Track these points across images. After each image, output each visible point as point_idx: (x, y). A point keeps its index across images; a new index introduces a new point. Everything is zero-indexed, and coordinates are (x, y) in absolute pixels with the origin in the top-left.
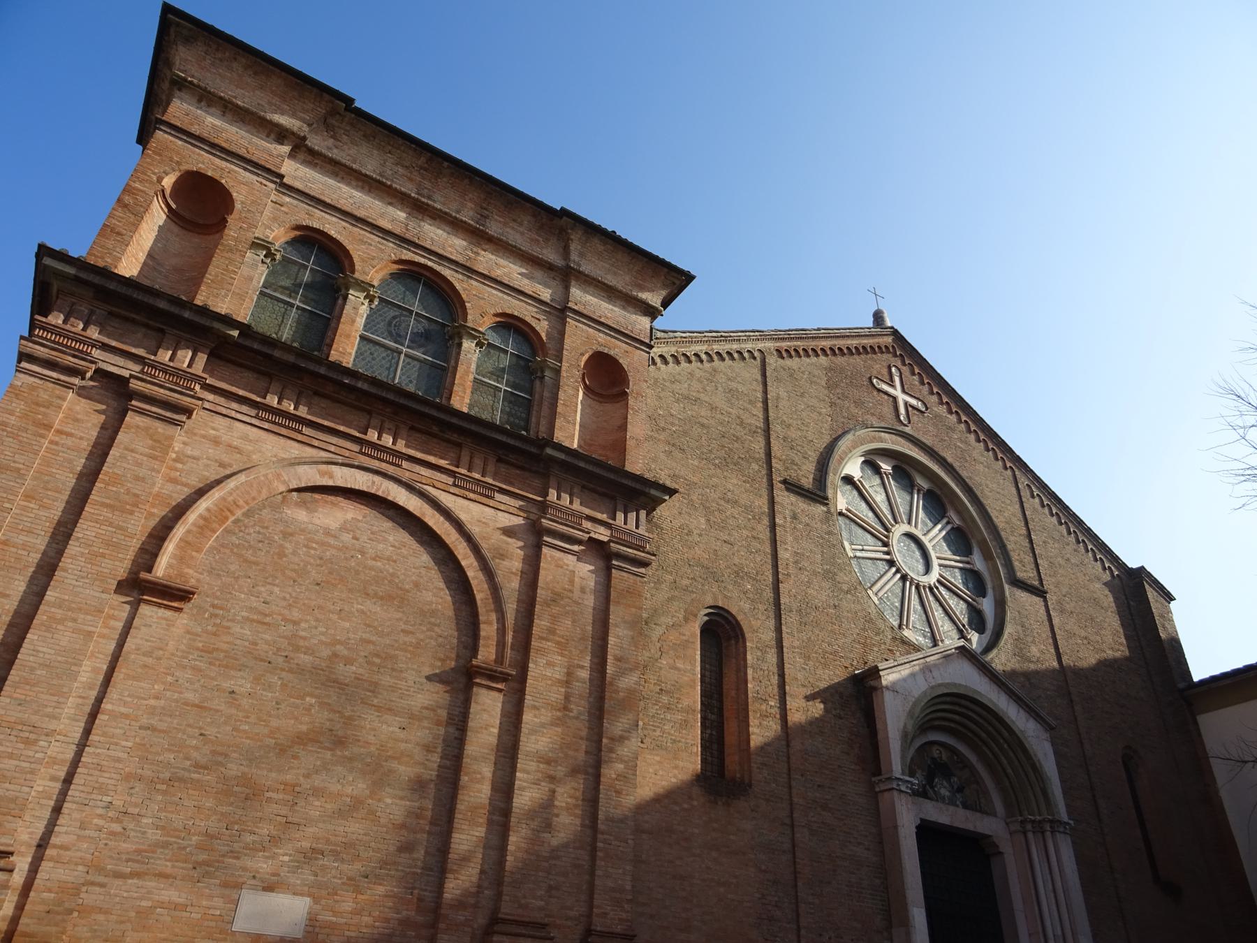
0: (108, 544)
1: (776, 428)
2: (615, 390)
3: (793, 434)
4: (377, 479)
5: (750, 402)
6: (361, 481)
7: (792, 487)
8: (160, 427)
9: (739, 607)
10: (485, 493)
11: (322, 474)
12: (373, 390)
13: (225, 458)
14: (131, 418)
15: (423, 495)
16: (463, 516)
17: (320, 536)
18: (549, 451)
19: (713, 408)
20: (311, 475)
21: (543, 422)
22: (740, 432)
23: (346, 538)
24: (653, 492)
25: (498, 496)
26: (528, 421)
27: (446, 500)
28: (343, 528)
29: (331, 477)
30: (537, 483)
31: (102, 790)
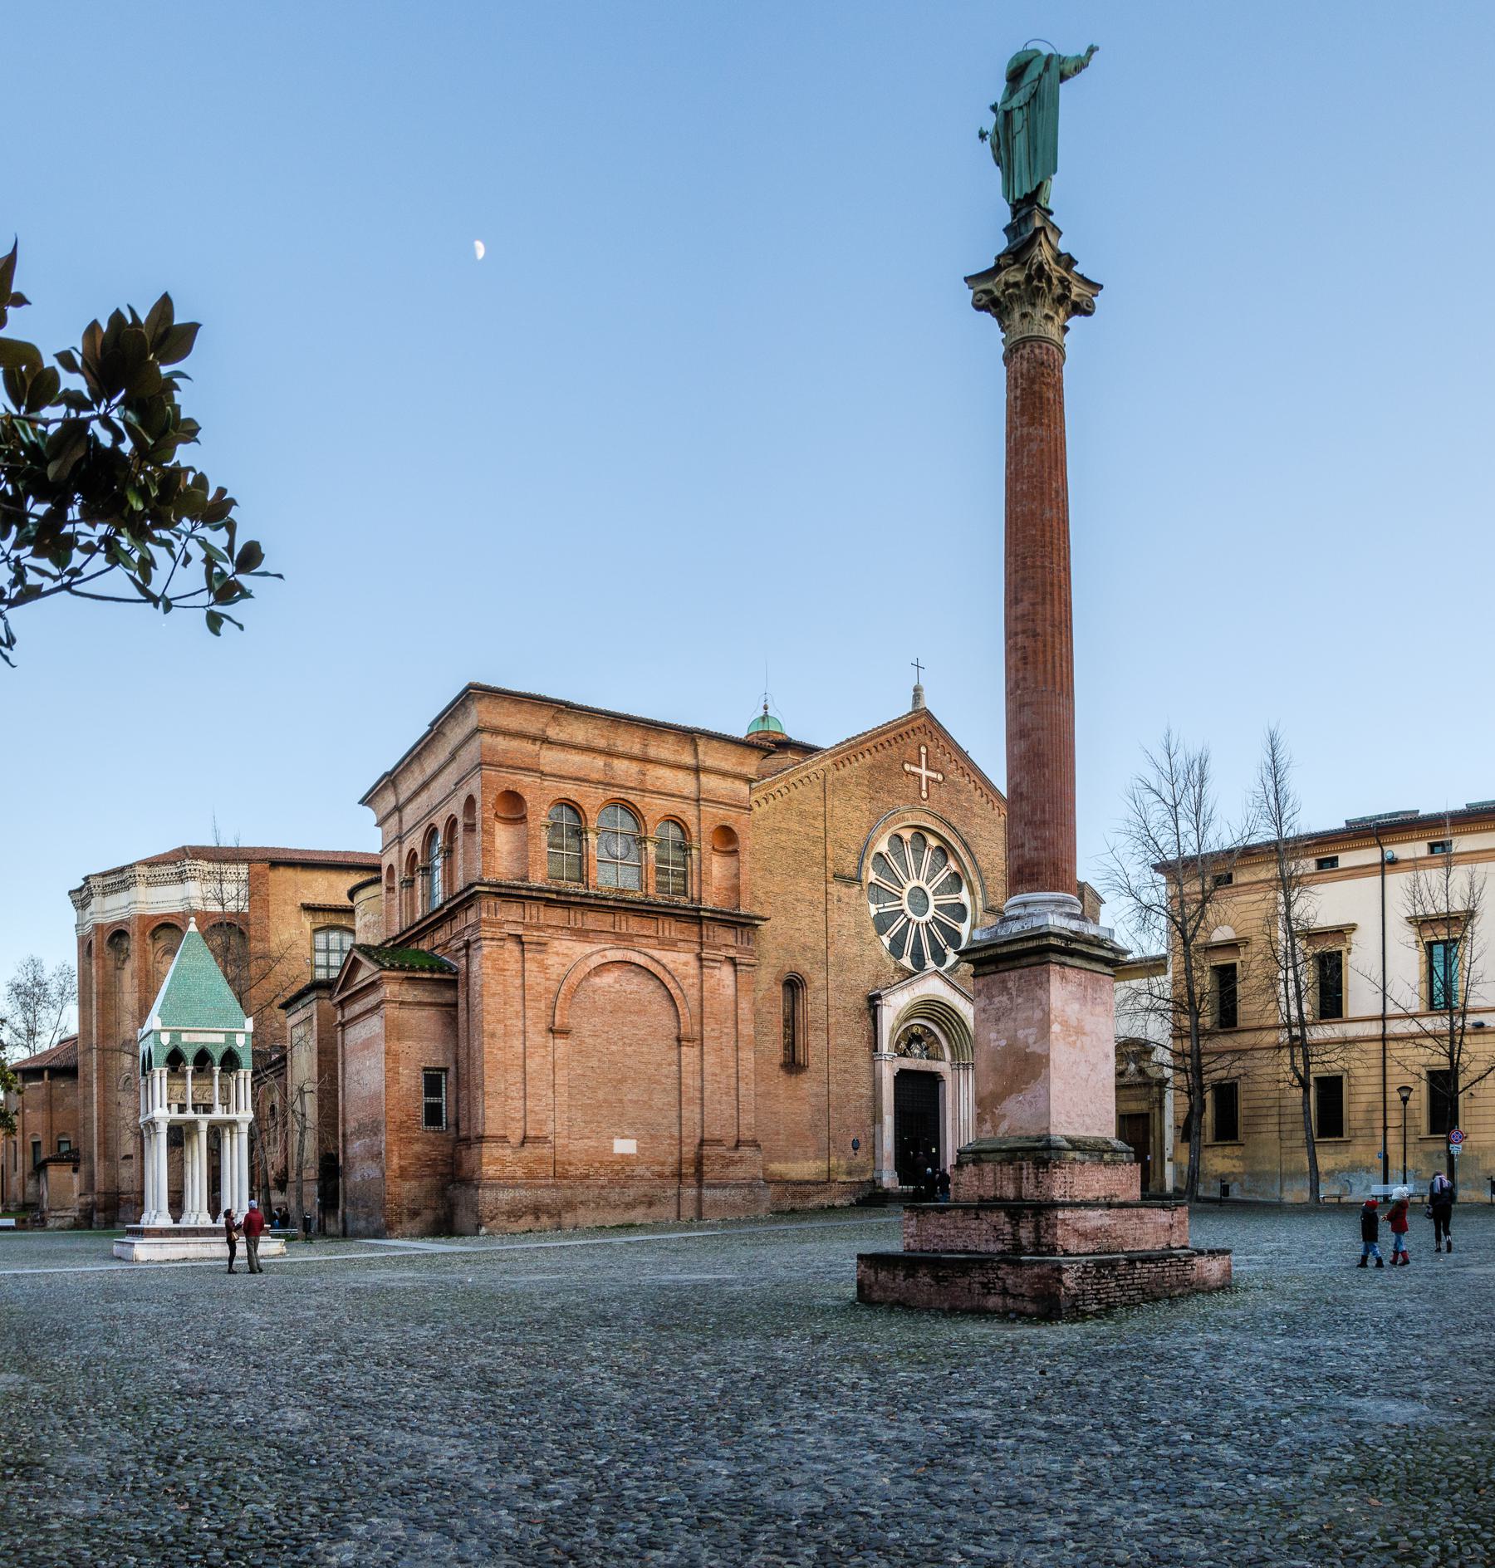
0: (538, 1017)
1: (831, 835)
2: (730, 848)
3: (842, 834)
5: (814, 818)
6: (618, 955)
7: (840, 877)
8: (539, 957)
9: (805, 967)
10: (670, 945)
11: (605, 956)
12: (617, 904)
13: (564, 961)
14: (528, 955)
16: (664, 961)
18: (702, 913)
19: (789, 831)
20: (597, 960)
21: (695, 887)
22: (807, 844)
24: (757, 922)
25: (680, 944)
26: (685, 886)
27: (656, 954)
29: (605, 956)
30: (696, 929)
31: (564, 1112)
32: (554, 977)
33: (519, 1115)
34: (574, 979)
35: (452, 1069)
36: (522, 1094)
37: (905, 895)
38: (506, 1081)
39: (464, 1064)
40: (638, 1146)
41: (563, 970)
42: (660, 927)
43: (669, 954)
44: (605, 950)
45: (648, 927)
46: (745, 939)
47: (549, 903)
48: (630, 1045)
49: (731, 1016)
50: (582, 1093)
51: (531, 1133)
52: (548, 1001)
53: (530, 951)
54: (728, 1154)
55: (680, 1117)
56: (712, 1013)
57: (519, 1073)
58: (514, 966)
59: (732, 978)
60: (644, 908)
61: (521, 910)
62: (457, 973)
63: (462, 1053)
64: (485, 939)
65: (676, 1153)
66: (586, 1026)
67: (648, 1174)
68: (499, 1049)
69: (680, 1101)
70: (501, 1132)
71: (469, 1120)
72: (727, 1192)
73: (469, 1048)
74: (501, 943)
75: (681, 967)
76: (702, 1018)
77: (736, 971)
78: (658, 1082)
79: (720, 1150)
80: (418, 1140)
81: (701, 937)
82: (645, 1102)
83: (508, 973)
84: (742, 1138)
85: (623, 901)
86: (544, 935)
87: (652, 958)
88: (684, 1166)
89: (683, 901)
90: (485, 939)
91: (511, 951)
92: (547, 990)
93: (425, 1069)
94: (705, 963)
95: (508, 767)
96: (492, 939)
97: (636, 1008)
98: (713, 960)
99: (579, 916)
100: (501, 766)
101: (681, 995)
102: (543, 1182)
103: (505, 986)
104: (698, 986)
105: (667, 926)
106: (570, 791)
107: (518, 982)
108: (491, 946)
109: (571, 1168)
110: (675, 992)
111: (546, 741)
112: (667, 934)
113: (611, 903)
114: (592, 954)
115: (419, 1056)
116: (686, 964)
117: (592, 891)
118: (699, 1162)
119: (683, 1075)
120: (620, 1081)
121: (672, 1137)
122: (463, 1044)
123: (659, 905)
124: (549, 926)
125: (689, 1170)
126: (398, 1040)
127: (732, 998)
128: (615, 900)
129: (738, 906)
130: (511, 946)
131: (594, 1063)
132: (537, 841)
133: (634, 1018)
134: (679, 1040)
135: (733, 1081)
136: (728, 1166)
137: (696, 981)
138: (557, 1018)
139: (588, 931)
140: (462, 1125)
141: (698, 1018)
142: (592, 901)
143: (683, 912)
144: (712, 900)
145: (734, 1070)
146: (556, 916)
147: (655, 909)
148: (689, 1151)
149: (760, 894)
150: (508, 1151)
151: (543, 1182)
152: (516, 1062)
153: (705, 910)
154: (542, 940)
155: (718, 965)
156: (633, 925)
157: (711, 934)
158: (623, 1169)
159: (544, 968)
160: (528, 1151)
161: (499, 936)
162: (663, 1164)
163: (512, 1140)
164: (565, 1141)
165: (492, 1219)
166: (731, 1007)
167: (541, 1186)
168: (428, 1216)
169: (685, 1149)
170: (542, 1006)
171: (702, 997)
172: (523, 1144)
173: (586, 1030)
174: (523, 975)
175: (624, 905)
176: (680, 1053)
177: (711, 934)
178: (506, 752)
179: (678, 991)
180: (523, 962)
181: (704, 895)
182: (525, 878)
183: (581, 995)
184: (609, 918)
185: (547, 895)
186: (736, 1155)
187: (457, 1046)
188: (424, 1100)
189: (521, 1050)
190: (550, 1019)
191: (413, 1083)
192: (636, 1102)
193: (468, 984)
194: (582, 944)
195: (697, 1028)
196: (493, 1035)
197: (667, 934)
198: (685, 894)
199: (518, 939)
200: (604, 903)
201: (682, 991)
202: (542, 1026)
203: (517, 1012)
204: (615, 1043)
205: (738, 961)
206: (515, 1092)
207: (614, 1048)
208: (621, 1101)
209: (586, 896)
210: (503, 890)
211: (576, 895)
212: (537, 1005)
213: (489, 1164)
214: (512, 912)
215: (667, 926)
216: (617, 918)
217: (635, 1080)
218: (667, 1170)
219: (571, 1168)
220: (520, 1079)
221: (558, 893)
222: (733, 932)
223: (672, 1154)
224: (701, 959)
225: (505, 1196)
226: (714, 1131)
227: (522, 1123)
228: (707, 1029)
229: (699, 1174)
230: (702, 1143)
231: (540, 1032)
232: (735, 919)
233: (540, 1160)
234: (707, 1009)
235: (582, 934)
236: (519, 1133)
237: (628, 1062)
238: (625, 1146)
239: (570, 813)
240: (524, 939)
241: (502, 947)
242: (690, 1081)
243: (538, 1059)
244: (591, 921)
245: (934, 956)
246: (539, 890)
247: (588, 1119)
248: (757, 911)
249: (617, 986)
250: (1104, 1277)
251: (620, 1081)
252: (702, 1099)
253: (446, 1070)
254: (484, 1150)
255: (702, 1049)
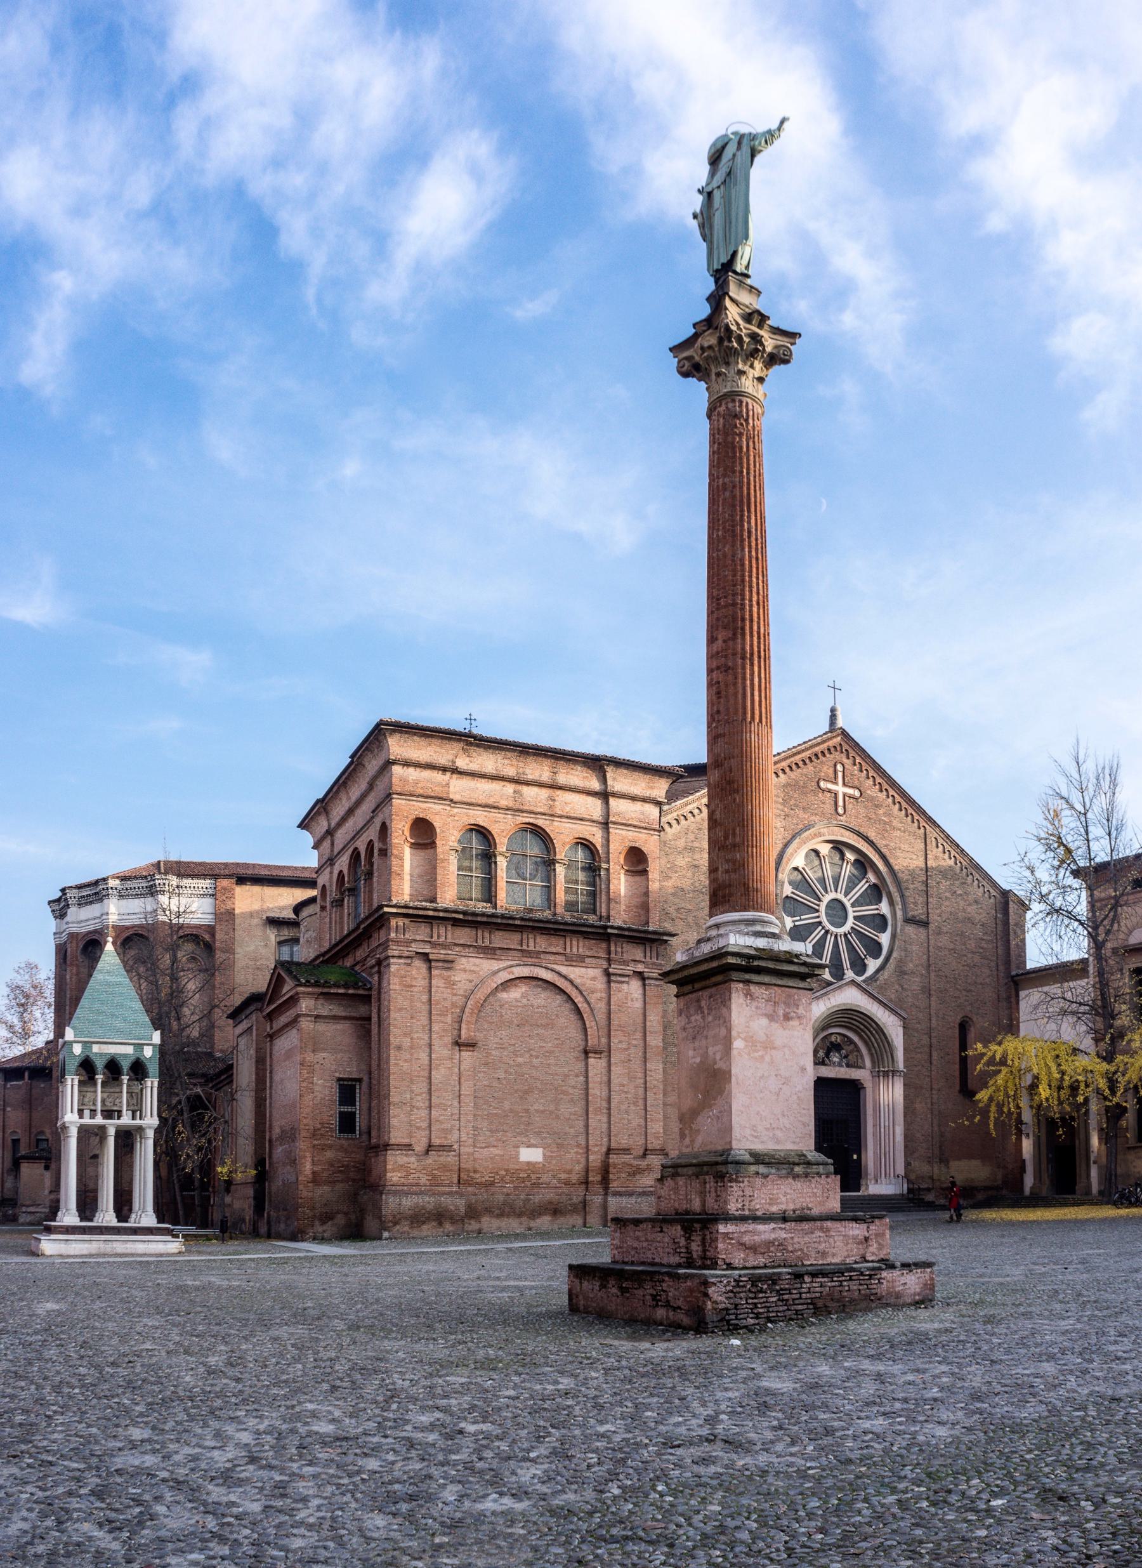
0: (444, 1030)
4: (532, 968)
6: (525, 971)
8: (445, 973)
10: (578, 960)
14: (435, 972)
15: (552, 970)
16: (572, 977)
17: (514, 1003)
18: (609, 931)
20: (504, 976)
21: (603, 905)
23: (524, 1001)
24: (665, 938)
25: (588, 960)
26: (594, 904)
27: (564, 970)
28: (522, 997)
30: (604, 945)
32: (461, 992)
33: (425, 1124)
34: (480, 995)
35: (366, 1079)
36: (427, 1104)
37: (823, 908)
38: (412, 1091)
39: (375, 1075)
40: (544, 1155)
41: (470, 986)
42: (568, 943)
43: (577, 970)
44: (512, 966)
45: (556, 945)
46: (654, 954)
47: (456, 923)
48: (537, 1057)
49: (640, 1028)
50: (486, 1102)
51: (436, 1141)
52: (455, 1016)
53: (437, 968)
54: (636, 1163)
55: (587, 1126)
56: (620, 1026)
57: (425, 1084)
58: (421, 982)
59: (640, 991)
60: (551, 926)
61: (428, 930)
62: (370, 989)
63: (374, 1063)
64: (393, 957)
65: (583, 1160)
66: (491, 1039)
67: (555, 1181)
68: (406, 1061)
69: (587, 1111)
70: (406, 1141)
71: (379, 1129)
72: (633, 1200)
73: (379, 1060)
74: (409, 961)
75: (589, 982)
76: (609, 1030)
77: (644, 985)
78: (563, 1092)
79: (626, 1158)
80: (330, 1147)
81: (609, 953)
82: (551, 1113)
83: (415, 989)
84: (650, 1147)
85: (530, 920)
86: (452, 953)
87: (559, 974)
88: (591, 1174)
89: (592, 919)
90: (393, 957)
91: (418, 969)
92: (454, 1005)
93: (339, 1079)
94: (613, 978)
95: (418, 796)
96: (400, 957)
97: (543, 1021)
98: (621, 975)
99: (487, 935)
100: (411, 795)
101: (588, 1009)
102: (447, 1189)
103: (412, 1001)
104: (605, 1001)
105: (575, 943)
106: (481, 817)
107: (425, 998)
108: (399, 964)
109: (477, 1176)
110: (582, 1006)
111: (455, 771)
112: (575, 950)
113: (517, 922)
114: (499, 971)
115: (333, 1068)
116: (594, 979)
117: (499, 911)
118: (605, 1171)
119: (590, 1085)
120: (526, 1092)
121: (578, 1145)
122: (375, 1057)
123: (566, 924)
124: (456, 945)
125: (594, 1178)
126: (313, 1051)
127: (641, 1011)
128: (522, 919)
129: (647, 923)
130: (418, 963)
131: (502, 1075)
132: (445, 864)
133: (541, 1031)
134: (586, 1053)
135: (641, 1091)
136: (634, 1174)
137: (604, 995)
138: (463, 1032)
139: (495, 949)
140: (374, 1133)
141: (606, 1031)
142: (499, 921)
143: (590, 930)
144: (620, 917)
145: (642, 1081)
146: (464, 935)
147: (562, 927)
148: (595, 1159)
149: (672, 910)
150: (413, 1159)
151: (447, 1189)
152: (422, 1073)
153: (612, 927)
154: (450, 958)
155: (626, 979)
156: (540, 943)
157: (619, 950)
158: (529, 1176)
159: (451, 984)
160: (432, 1159)
161: (406, 954)
162: (570, 1172)
163: (417, 1149)
164: (470, 1150)
165: (395, 1224)
166: (640, 1020)
167: (445, 1193)
168: (340, 1220)
169: (591, 1158)
170: (449, 1019)
171: (609, 1010)
172: (427, 1152)
173: (493, 1042)
174: (430, 991)
175: (531, 924)
176: (587, 1064)
177: (619, 950)
178: (416, 782)
179: (586, 1005)
180: (430, 979)
181: (612, 913)
182: (433, 900)
183: (488, 1009)
184: (516, 937)
185: (454, 915)
186: (643, 1164)
187: (370, 1056)
188: (337, 1109)
189: (427, 1062)
190: (455, 1032)
191: (327, 1092)
192: (543, 1112)
193: (379, 1000)
194: (489, 961)
195: (604, 1040)
196: (399, 1048)
197: (575, 950)
198: (594, 912)
199: (425, 957)
200: (511, 922)
201: (589, 1004)
202: (448, 1039)
203: (424, 1026)
204: (522, 1056)
205: (646, 975)
206: (421, 1102)
207: (520, 1060)
208: (527, 1111)
209: (493, 916)
210: (411, 911)
211: (483, 915)
212: (442, 1018)
213: (393, 1171)
214: (421, 932)
215: (575, 943)
216: (525, 936)
217: (541, 1091)
218: (574, 1178)
219: (477, 1176)
220: (425, 1090)
221: (465, 913)
222: (641, 947)
223: (579, 1162)
224: (608, 974)
225: (408, 1202)
226: (621, 1140)
227: (427, 1132)
228: (614, 1040)
229: (605, 1181)
230: (609, 1150)
231: (446, 1046)
232: (642, 935)
233: (445, 1168)
234: (614, 1022)
235: (489, 952)
236: (424, 1142)
237: (534, 1073)
238: (531, 1155)
239: (480, 837)
240: (431, 957)
241: (409, 965)
242: (597, 1091)
243: (443, 1071)
244: (499, 939)
245: (853, 966)
246: (446, 910)
247: (493, 1127)
248: (668, 926)
249: (524, 1001)
250: (761, 1291)
251: (526, 1092)
252: (609, 1109)
253: (360, 1080)
254: (389, 1158)
255: (609, 1061)
